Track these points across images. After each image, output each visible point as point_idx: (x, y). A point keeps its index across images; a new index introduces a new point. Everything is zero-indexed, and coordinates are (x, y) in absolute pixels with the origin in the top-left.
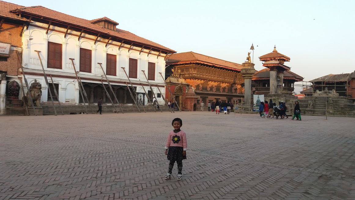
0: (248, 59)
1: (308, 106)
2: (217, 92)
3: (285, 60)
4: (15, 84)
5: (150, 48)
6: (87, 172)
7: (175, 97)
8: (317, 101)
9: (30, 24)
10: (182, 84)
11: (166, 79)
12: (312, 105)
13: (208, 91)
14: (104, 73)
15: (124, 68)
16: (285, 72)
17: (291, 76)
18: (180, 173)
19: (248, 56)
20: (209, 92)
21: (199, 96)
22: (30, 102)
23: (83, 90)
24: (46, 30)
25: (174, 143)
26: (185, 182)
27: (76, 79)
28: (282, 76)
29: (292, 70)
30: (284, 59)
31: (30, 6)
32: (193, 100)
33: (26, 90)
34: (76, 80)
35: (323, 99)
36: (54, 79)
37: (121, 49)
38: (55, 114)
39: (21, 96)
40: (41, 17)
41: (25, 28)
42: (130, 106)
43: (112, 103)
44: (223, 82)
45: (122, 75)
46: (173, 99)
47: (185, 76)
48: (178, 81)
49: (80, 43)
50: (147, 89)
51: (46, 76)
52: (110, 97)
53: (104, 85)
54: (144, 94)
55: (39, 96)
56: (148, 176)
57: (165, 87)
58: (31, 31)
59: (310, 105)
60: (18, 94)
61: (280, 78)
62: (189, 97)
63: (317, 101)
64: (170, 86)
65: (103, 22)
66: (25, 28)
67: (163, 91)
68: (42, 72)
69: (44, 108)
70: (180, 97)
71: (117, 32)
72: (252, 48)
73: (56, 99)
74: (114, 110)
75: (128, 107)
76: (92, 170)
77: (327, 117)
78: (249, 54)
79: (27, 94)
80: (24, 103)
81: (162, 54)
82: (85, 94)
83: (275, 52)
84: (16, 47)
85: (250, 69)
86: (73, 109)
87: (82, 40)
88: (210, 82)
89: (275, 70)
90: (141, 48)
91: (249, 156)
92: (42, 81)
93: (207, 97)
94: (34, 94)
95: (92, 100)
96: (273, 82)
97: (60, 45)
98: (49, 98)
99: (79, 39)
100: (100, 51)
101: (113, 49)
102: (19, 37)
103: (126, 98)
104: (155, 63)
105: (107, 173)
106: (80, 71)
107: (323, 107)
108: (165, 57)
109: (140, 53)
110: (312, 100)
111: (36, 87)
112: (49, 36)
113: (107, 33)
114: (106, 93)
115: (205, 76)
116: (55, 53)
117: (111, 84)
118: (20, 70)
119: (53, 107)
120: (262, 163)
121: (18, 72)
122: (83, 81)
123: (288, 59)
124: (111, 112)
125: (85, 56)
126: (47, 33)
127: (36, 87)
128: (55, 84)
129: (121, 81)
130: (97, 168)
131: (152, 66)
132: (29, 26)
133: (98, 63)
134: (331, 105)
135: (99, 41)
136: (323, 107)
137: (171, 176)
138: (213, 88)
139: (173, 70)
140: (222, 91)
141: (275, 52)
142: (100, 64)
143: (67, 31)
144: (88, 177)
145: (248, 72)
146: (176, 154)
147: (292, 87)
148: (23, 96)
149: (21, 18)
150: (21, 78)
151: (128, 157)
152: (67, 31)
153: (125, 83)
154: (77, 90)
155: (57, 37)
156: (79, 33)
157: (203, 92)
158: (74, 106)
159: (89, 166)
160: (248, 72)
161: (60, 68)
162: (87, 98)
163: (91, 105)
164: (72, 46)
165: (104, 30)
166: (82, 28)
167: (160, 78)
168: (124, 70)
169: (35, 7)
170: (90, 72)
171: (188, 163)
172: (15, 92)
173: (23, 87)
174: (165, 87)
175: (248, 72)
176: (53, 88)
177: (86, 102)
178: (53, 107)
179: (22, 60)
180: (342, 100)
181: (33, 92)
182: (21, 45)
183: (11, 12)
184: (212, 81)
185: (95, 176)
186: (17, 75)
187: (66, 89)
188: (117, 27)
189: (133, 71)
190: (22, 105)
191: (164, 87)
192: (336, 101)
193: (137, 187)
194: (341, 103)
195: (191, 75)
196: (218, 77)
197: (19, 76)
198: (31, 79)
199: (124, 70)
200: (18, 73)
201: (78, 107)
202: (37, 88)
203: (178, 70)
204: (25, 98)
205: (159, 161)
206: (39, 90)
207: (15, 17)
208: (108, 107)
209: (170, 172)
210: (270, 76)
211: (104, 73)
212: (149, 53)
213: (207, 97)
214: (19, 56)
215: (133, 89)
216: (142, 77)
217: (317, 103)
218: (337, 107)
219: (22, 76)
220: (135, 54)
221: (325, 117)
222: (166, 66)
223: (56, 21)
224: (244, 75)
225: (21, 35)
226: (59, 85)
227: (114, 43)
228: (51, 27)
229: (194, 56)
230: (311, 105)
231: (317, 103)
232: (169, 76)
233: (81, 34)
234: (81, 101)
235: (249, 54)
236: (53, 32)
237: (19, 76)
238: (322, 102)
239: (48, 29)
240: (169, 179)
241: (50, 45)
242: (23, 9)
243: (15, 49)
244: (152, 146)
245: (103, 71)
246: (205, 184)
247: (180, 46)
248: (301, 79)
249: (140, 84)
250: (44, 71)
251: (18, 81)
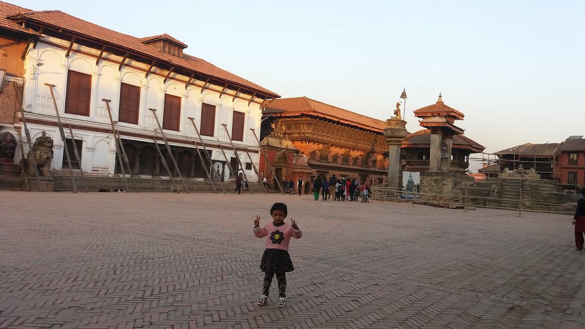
0: (397, 113)
1: (491, 193)
2: (344, 165)
3: (455, 118)
4: (9, 137)
5: (253, 93)
6: (126, 288)
7: (275, 169)
9: (40, 39)
10: (287, 149)
11: (261, 139)
12: (498, 192)
14: (160, 126)
15: (192, 119)
16: (454, 136)
17: (465, 143)
18: (282, 295)
19: (396, 109)
20: (331, 165)
21: (315, 170)
22: (33, 169)
23: (122, 153)
24: (67, 51)
25: (274, 243)
26: (291, 311)
27: (112, 133)
28: (450, 143)
29: (466, 134)
30: (453, 115)
31: (42, 10)
32: (305, 176)
33: (27, 149)
34: (112, 136)
35: (515, 183)
36: (74, 131)
37: (189, 88)
38: (73, 191)
39: (18, 159)
40: (59, 28)
41: (31, 45)
42: (200, 182)
43: (170, 176)
44: (354, 150)
45: (188, 129)
46: (271, 173)
47: (293, 136)
48: (281, 144)
49: (122, 74)
50: (229, 155)
51: (61, 126)
52: (166, 165)
53: (157, 146)
54: (224, 163)
55: (49, 159)
56: (229, 298)
57: (259, 152)
58: (41, 50)
59: (494, 192)
60: (13, 155)
61: (446, 146)
62: (298, 170)
64: (267, 151)
65: (162, 42)
66: (31, 45)
67: (256, 159)
68: (56, 120)
69: (55, 179)
70: (284, 170)
71: (184, 60)
72: (404, 95)
73: (77, 165)
74: (173, 188)
75: (196, 183)
76: (136, 285)
77: (521, 212)
78: (398, 105)
79: (28, 155)
80: (23, 170)
81: (256, 99)
82: (126, 159)
83: (440, 103)
84: (14, 76)
85: (398, 130)
86: (105, 182)
87: (125, 70)
88: (333, 149)
89: (439, 132)
90: (251, 97)
91: (396, 271)
92: (54, 134)
93: (328, 172)
94: (40, 157)
95: (137, 170)
96: (435, 152)
97: (89, 77)
98: (65, 164)
99: (120, 68)
100: (154, 89)
101: (176, 88)
102: (20, 60)
103: (193, 169)
104: (244, 113)
105: (160, 290)
106: (120, 120)
107: (514, 195)
108: (261, 104)
109: (220, 95)
110: (498, 184)
111: (45, 144)
112: (70, 61)
113: (167, 60)
114: (160, 158)
115: (325, 138)
116: (79, 89)
117: (170, 144)
118: (19, 115)
119: (72, 178)
120: (417, 284)
121: (14, 118)
122: (123, 137)
123: (460, 116)
124: (167, 190)
125: (130, 97)
126: (67, 56)
127: (45, 144)
128: (76, 141)
129: (188, 140)
130: (143, 283)
131: (239, 118)
132: (38, 43)
133: (150, 109)
134: (528, 194)
135: (153, 73)
136: (514, 195)
137: (268, 300)
139: (273, 126)
140: (351, 164)
141: (440, 103)
142: (154, 110)
143: (101, 54)
144: (128, 296)
145: (396, 134)
146: (277, 264)
147: (466, 161)
148: (21, 158)
149: (26, 29)
150: (20, 128)
151: (196, 267)
152: (101, 54)
153: (193, 143)
154: (112, 152)
155: (84, 63)
156: (120, 59)
157: (321, 164)
158: (106, 178)
159: (130, 278)
160: (395, 133)
161: (87, 114)
162: (128, 165)
163: (156, 178)
164: (107, 79)
165: (163, 56)
166: (126, 50)
167: (251, 138)
168: (193, 122)
169: (48, 12)
170: (136, 122)
171: (296, 278)
172: (8, 151)
173: (21, 142)
174: (259, 152)
175: (395, 133)
176: (73, 148)
177: (126, 173)
178: (72, 178)
179: (22, 98)
180: (546, 185)
181: (38, 153)
182: (23, 74)
183: (8, 18)
184: (337, 146)
185: (140, 294)
186: (13, 124)
187: (94, 149)
188: (185, 51)
189: (207, 125)
190: (19, 173)
191: (257, 152)
192: (536, 188)
193: (211, 315)
195: (302, 135)
197: (16, 125)
198: (36, 131)
199: (193, 122)
200: (15, 120)
201: (114, 179)
202: (46, 146)
203: (282, 125)
204: (25, 162)
205: (248, 274)
206: (48, 149)
207: (15, 27)
208: (163, 182)
209: (266, 292)
210: (432, 143)
211: (160, 126)
212: (236, 96)
214: (19, 92)
215: (206, 155)
216: (221, 134)
217: (505, 190)
218: (537, 196)
219: (22, 125)
220: (212, 97)
221: (518, 212)
222: (262, 118)
223: (83, 37)
224: (389, 139)
225: (23, 58)
226: (83, 142)
227: (179, 76)
228: (75, 46)
229: (308, 104)
230: (495, 193)
231: (506, 188)
232: (267, 135)
233: (124, 60)
234: (118, 169)
235: (398, 105)
236: (78, 55)
237: (16, 125)
238: (513, 187)
239: (70, 49)
240: (264, 304)
241: (72, 76)
242: (30, 14)
243: (12, 79)
244: (236, 249)
245: (196, 129)
246: (325, 314)
247: (287, 88)
248: (480, 149)
249: (219, 147)
250: (59, 117)
251: (14, 132)
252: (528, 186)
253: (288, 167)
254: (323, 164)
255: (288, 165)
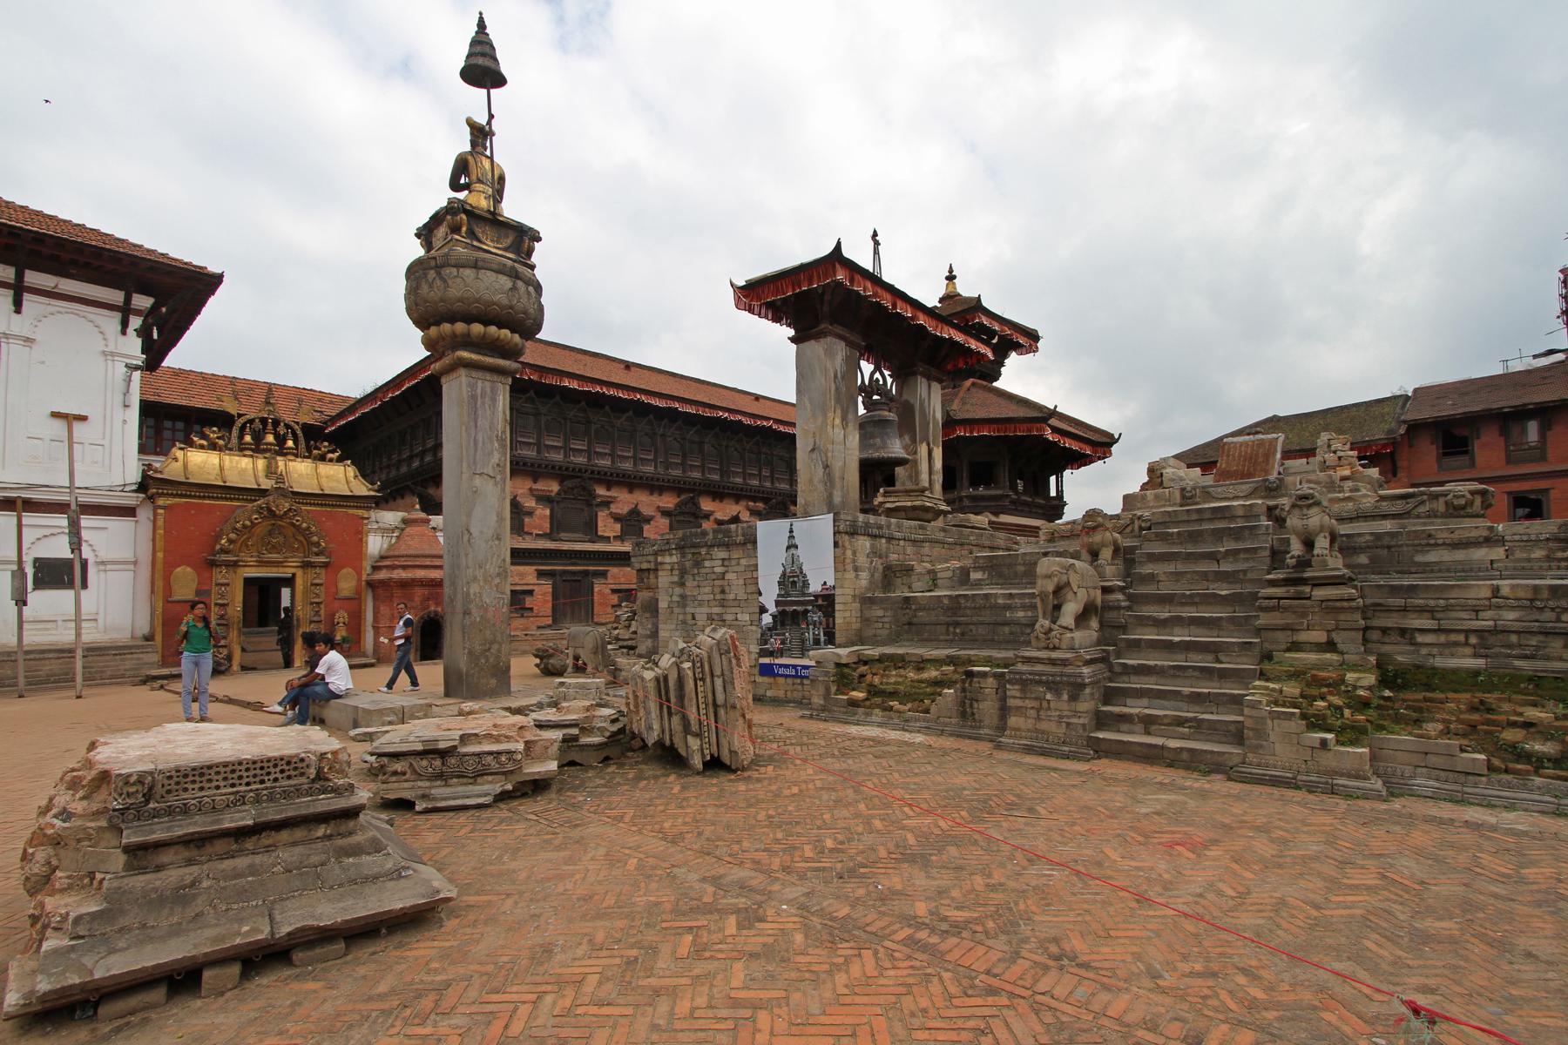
8: (1153, 558)
13: (607, 539)
21: (530, 569)
63: (1153, 558)
93: (603, 574)
110: (1094, 554)
134: (1329, 607)
138: (648, 520)
147: (1053, 493)
180: (1473, 527)
192: (1385, 554)
194: (1469, 571)
196: (668, 465)
213: (603, 574)
231: (1151, 578)
252: (1322, 543)
253: (326, 565)
254: (566, 546)
255: (323, 559)
